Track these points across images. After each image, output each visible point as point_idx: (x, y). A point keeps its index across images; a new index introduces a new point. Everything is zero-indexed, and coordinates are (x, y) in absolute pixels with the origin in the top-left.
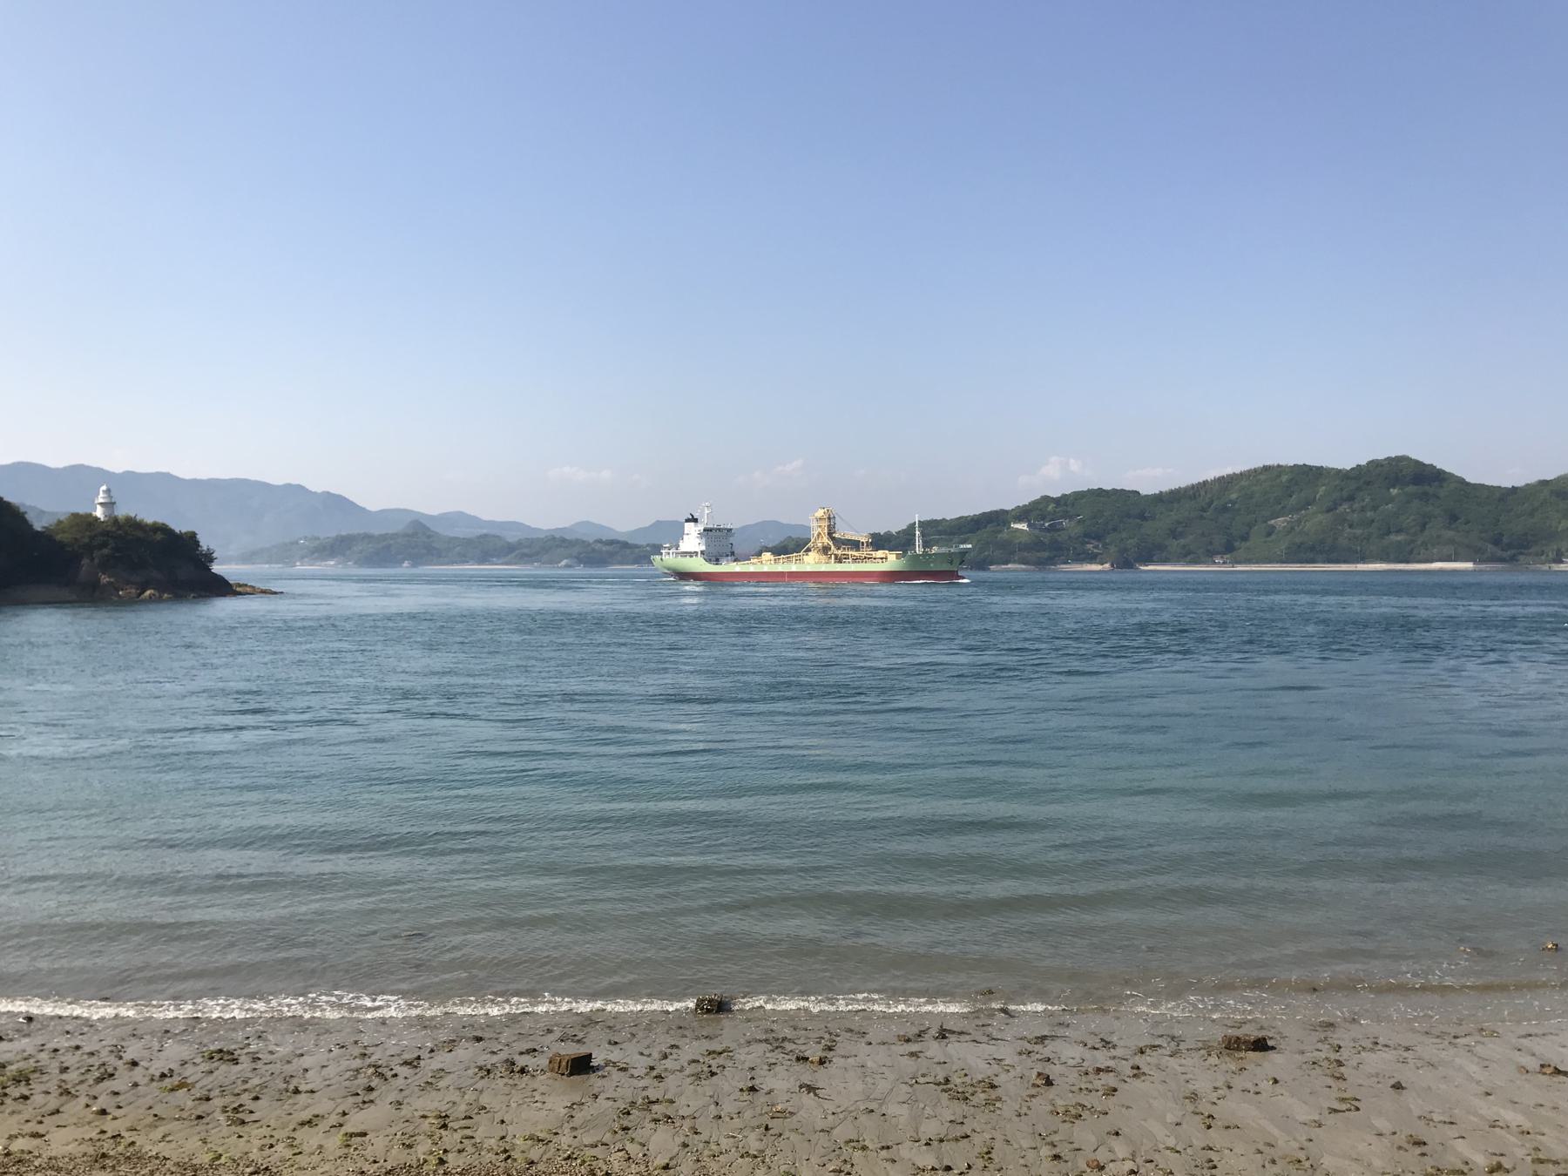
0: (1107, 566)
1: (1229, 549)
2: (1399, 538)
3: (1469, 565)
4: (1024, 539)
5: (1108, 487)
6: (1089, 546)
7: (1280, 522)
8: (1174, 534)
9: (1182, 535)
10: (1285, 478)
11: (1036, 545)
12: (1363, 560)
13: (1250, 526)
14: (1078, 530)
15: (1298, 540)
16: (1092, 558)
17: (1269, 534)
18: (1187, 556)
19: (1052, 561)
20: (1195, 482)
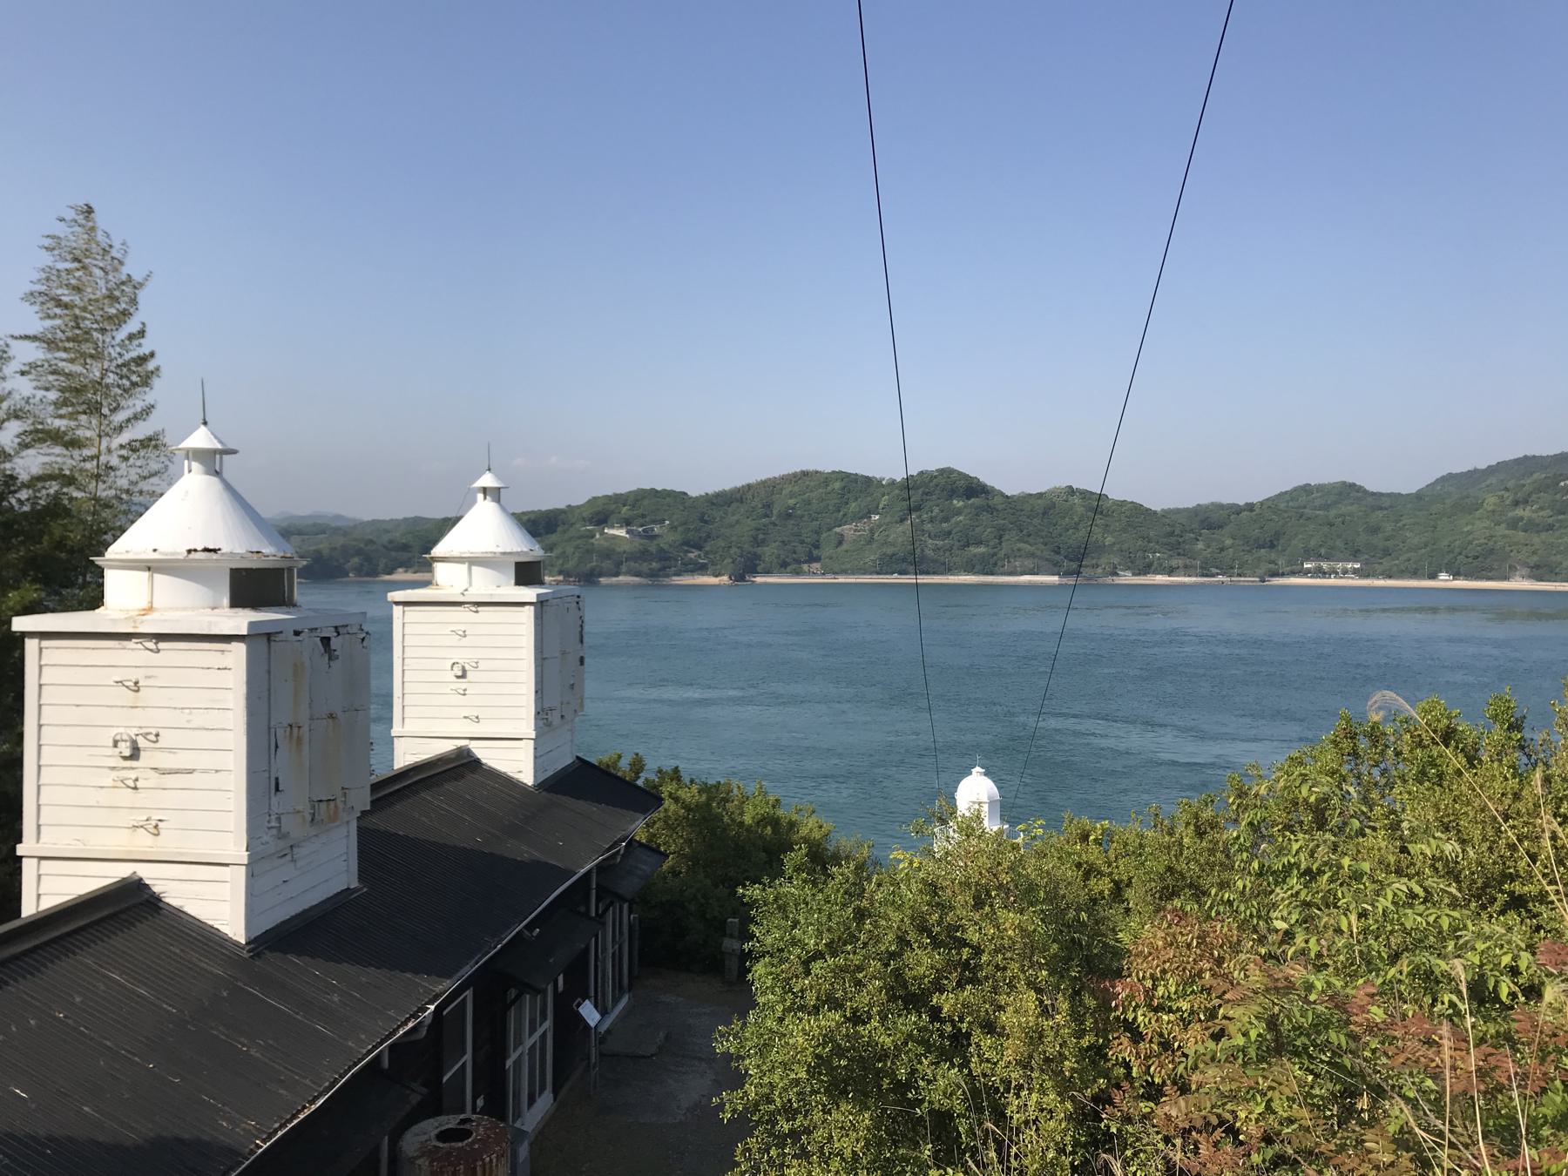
0: (725, 578)
1: (812, 559)
2: (982, 549)
3: (1055, 579)
4: (627, 547)
5: (659, 488)
6: (692, 555)
7: (847, 530)
8: (757, 542)
9: (763, 543)
10: (837, 485)
11: (643, 555)
12: (949, 570)
13: (818, 533)
14: (676, 537)
15: (890, 551)
16: (701, 569)
17: (840, 543)
18: (783, 566)
19: (662, 572)
20: (739, 485)
